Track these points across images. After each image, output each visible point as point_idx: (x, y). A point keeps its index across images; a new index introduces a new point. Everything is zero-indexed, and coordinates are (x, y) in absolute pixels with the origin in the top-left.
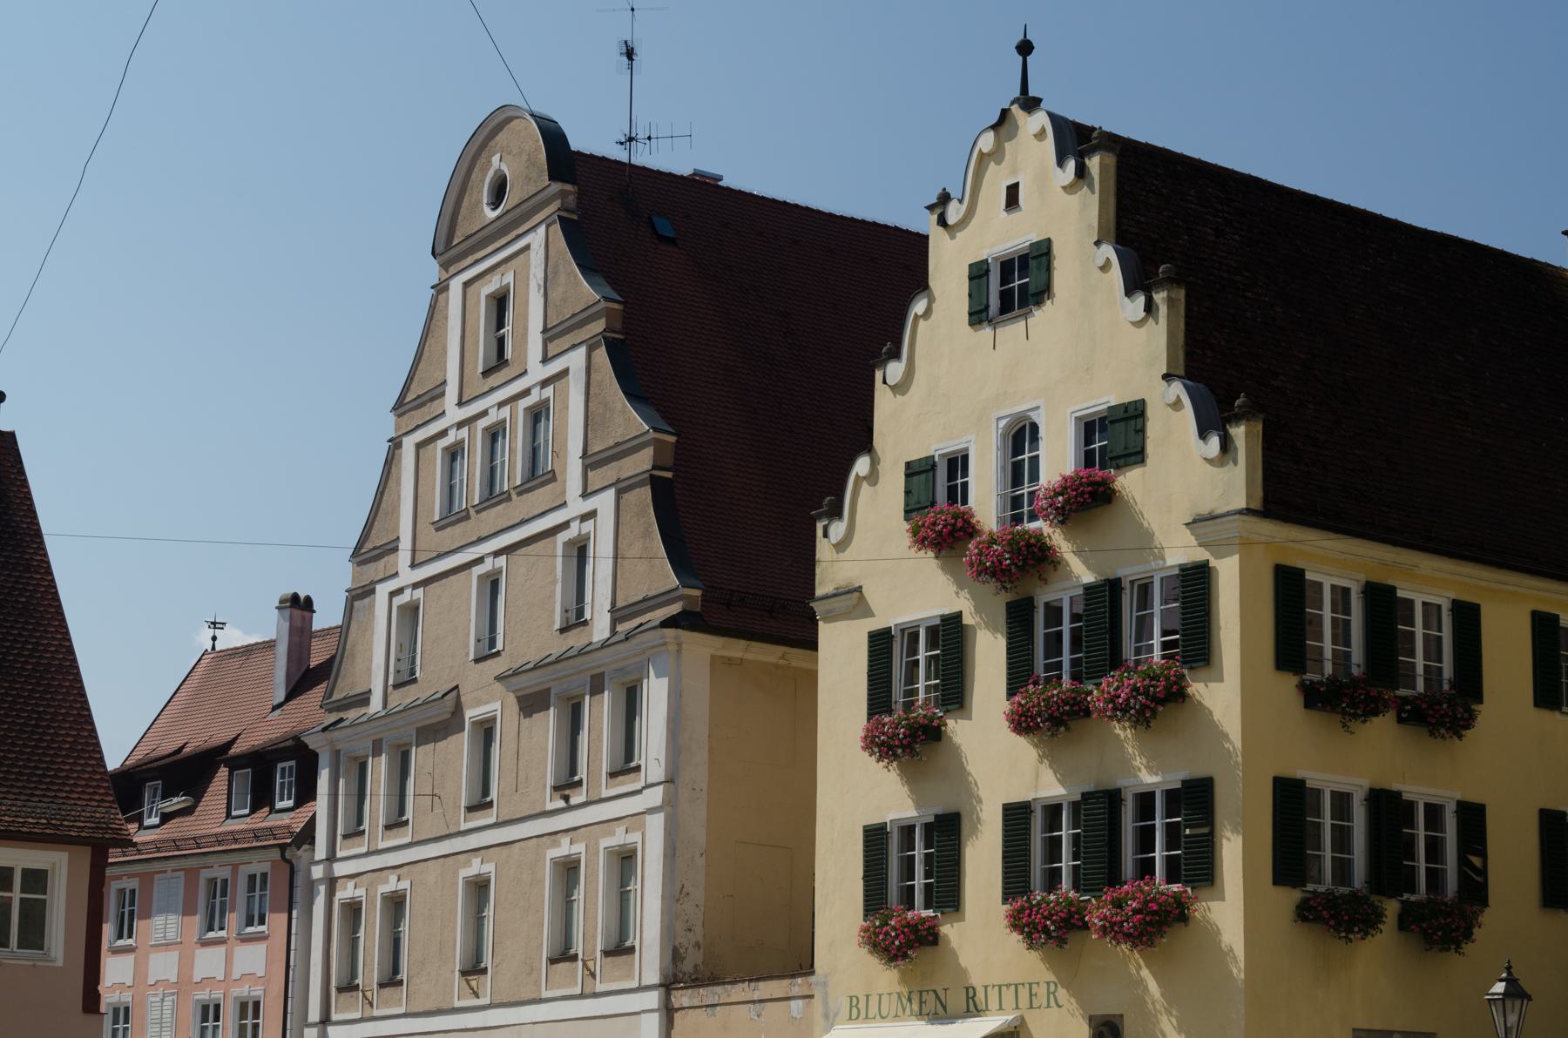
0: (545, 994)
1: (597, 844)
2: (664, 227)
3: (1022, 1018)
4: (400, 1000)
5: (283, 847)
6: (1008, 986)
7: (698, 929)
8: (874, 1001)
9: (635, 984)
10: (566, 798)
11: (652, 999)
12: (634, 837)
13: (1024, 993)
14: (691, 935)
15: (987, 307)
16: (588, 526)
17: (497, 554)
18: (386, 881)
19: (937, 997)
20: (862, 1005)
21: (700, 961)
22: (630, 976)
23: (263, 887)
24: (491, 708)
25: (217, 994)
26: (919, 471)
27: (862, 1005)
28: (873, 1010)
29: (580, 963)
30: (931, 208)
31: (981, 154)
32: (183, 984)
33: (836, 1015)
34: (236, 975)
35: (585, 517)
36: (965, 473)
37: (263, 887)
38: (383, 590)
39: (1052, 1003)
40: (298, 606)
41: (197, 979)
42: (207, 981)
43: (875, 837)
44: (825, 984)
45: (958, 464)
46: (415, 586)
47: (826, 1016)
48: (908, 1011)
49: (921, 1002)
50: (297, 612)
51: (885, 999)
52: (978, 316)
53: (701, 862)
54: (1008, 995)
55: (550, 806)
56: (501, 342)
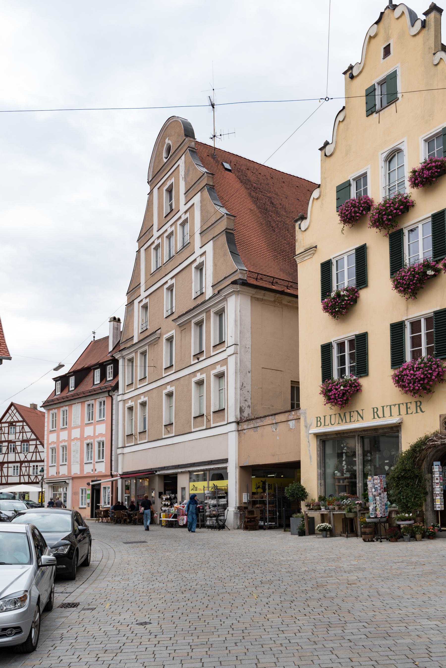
0: (193, 430)
1: (210, 373)
2: (227, 166)
3: (402, 418)
4: (146, 437)
5: (109, 391)
6: (395, 405)
7: (249, 400)
8: (328, 418)
9: (226, 423)
10: (198, 359)
11: (233, 427)
12: (224, 368)
13: (403, 408)
14: (246, 403)
15: (375, 105)
16: (203, 258)
17: (172, 278)
18: (140, 399)
19: (358, 413)
20: (322, 421)
21: (250, 413)
22: (224, 420)
23: (104, 404)
24: (173, 332)
25: (92, 441)
26: (343, 189)
27: (322, 421)
28: (328, 422)
29: (205, 417)
30: (345, 73)
31: (370, 37)
32: (82, 438)
33: (311, 425)
34: (97, 434)
35: (201, 255)
36: (365, 184)
37: (104, 404)
38: (136, 302)
39: (419, 410)
40: (115, 320)
41: (85, 436)
42: (89, 437)
43: (326, 349)
44: (305, 413)
45: (362, 179)
46: (146, 298)
47: (306, 427)
48: (344, 421)
49: (350, 417)
50: (115, 323)
51: (333, 417)
52: (371, 110)
53: (249, 375)
54: (395, 410)
55: (192, 363)
56: (171, 206)
